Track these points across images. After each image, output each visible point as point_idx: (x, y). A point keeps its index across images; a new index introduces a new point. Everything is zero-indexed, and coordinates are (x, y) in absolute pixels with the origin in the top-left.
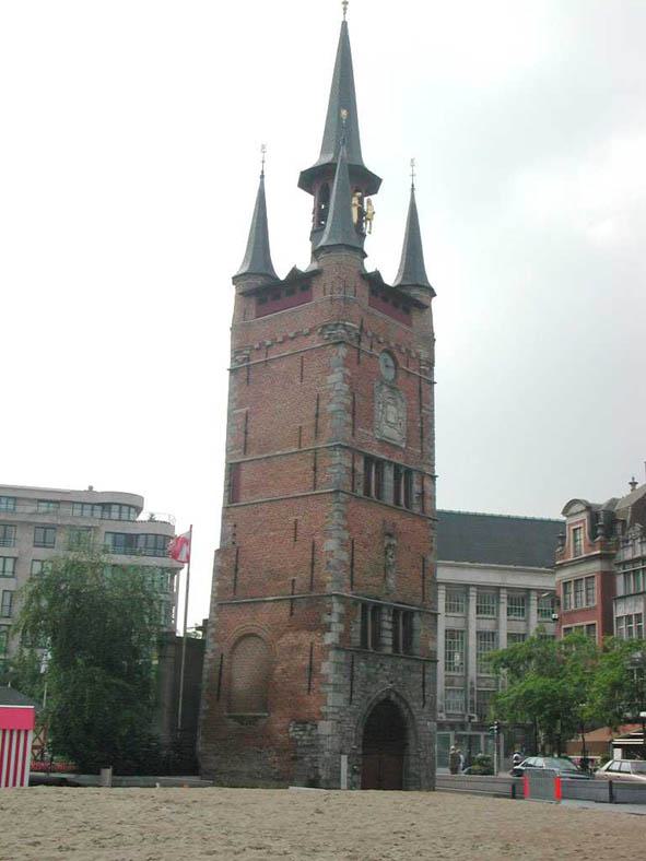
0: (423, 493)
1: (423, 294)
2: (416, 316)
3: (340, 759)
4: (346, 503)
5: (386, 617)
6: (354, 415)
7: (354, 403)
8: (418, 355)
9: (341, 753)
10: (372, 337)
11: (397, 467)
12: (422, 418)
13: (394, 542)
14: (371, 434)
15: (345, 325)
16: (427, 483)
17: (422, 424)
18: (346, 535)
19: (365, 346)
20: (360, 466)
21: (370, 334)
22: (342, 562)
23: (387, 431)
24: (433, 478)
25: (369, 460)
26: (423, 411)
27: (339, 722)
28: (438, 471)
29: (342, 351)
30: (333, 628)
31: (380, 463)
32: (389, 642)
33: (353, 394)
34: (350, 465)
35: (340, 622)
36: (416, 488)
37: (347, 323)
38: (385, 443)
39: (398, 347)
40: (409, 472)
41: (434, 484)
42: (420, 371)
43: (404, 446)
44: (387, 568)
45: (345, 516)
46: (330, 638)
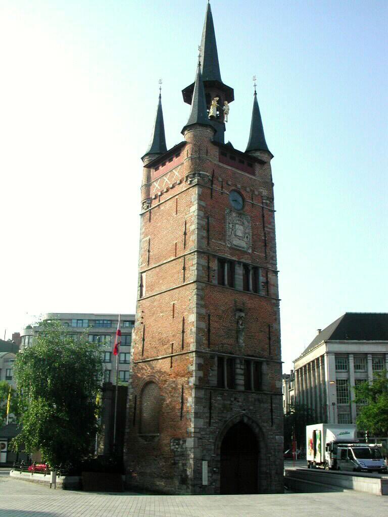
2: (257, 167)
3: (201, 464)
5: (238, 366)
6: (208, 231)
7: (208, 223)
8: (260, 193)
9: (203, 460)
11: (246, 266)
12: (265, 233)
13: (243, 315)
14: (224, 244)
16: (270, 276)
17: (265, 237)
20: (215, 265)
23: (236, 242)
24: (276, 272)
25: (222, 261)
26: (266, 229)
27: (201, 439)
31: (232, 264)
32: (242, 382)
34: (206, 264)
36: (262, 279)
39: (245, 188)
41: (277, 277)
42: (263, 203)
43: (250, 251)
44: (238, 332)
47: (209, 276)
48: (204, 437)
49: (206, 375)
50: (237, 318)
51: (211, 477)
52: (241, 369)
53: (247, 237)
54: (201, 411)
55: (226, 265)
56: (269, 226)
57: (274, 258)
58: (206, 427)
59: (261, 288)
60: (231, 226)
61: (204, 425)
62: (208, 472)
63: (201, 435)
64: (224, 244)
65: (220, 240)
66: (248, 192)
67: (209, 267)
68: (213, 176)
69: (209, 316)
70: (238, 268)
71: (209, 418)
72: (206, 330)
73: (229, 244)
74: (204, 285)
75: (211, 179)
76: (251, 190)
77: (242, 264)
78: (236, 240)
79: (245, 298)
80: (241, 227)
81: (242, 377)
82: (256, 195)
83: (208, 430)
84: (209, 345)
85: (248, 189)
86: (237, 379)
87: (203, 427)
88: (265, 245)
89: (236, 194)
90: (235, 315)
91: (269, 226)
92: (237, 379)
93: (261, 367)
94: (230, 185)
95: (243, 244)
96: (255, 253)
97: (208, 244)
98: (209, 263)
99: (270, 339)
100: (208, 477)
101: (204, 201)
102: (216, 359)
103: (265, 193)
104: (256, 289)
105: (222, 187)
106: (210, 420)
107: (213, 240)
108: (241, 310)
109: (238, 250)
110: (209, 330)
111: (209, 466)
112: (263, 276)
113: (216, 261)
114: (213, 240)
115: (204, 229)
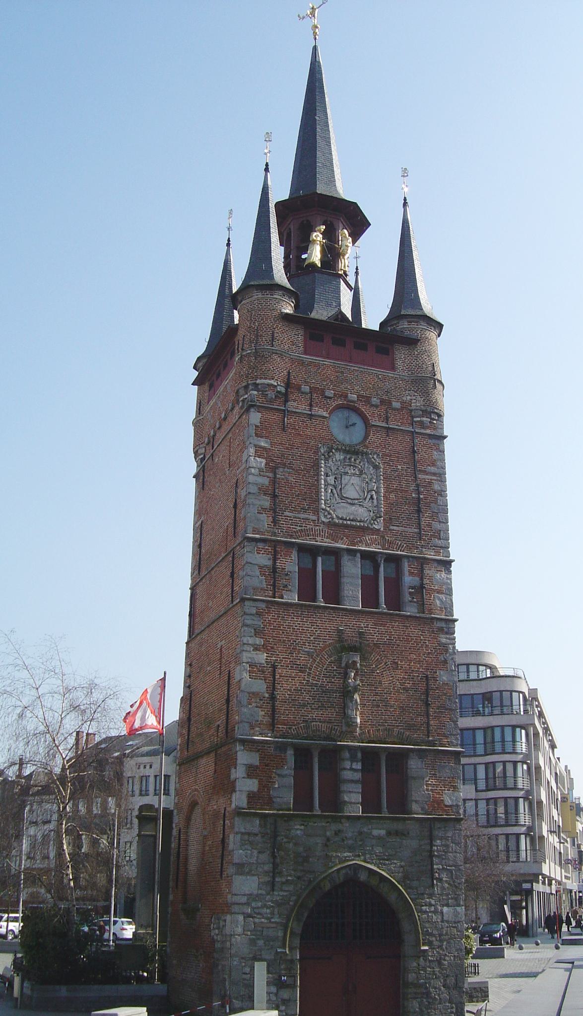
0: (422, 587)
1: (414, 325)
2: (401, 356)
3: (252, 968)
4: (258, 614)
5: (347, 764)
6: (274, 496)
7: (274, 481)
8: (406, 406)
9: (257, 958)
10: (311, 393)
12: (418, 486)
14: (315, 518)
15: (256, 385)
17: (419, 493)
18: (262, 657)
19: (297, 405)
20: (291, 564)
21: (306, 388)
22: (255, 694)
23: (343, 511)
24: (447, 564)
25: (310, 552)
27: (250, 916)
28: (455, 552)
29: (255, 417)
30: (239, 785)
33: (274, 470)
34: (270, 563)
35: (249, 776)
36: (409, 580)
37: (258, 381)
38: (338, 528)
40: (395, 561)
43: (379, 525)
45: (258, 632)
46: (239, 800)
47: (274, 586)
48: (259, 914)
49: (265, 786)
50: (343, 665)
51: (276, 994)
52: (351, 769)
53: (372, 498)
54: (254, 860)
55: (320, 559)
56: (432, 469)
57: (440, 536)
58: (264, 892)
59: (407, 598)
60: (331, 480)
61: (259, 888)
62: (268, 984)
63: (253, 908)
64: (315, 518)
65: (305, 510)
66: (377, 406)
67: (274, 570)
68: (288, 385)
69: (274, 667)
70: (349, 564)
71: (271, 874)
72: (267, 695)
73: (325, 516)
74: (263, 605)
75: (283, 390)
76: (382, 402)
77: (358, 555)
78: (343, 507)
79: (366, 625)
80: (355, 480)
81: (359, 788)
82: (395, 409)
83: (268, 897)
84: (272, 726)
85: (375, 401)
86: (344, 792)
87: (255, 892)
88: (419, 511)
89: (346, 413)
90: (340, 660)
91: (432, 469)
92: (344, 792)
93: (407, 763)
94: (330, 398)
95: (362, 513)
96: (392, 527)
97: (275, 522)
98: (275, 560)
99: (427, 705)
100: (268, 993)
101: (267, 437)
102: (290, 752)
103: (418, 403)
104: (395, 602)
105: (311, 405)
106: (274, 877)
107: (287, 513)
108: (354, 649)
109: (347, 526)
110: (273, 698)
111: (268, 972)
112: (411, 574)
113: (294, 555)
114: (287, 513)
115: (265, 494)
